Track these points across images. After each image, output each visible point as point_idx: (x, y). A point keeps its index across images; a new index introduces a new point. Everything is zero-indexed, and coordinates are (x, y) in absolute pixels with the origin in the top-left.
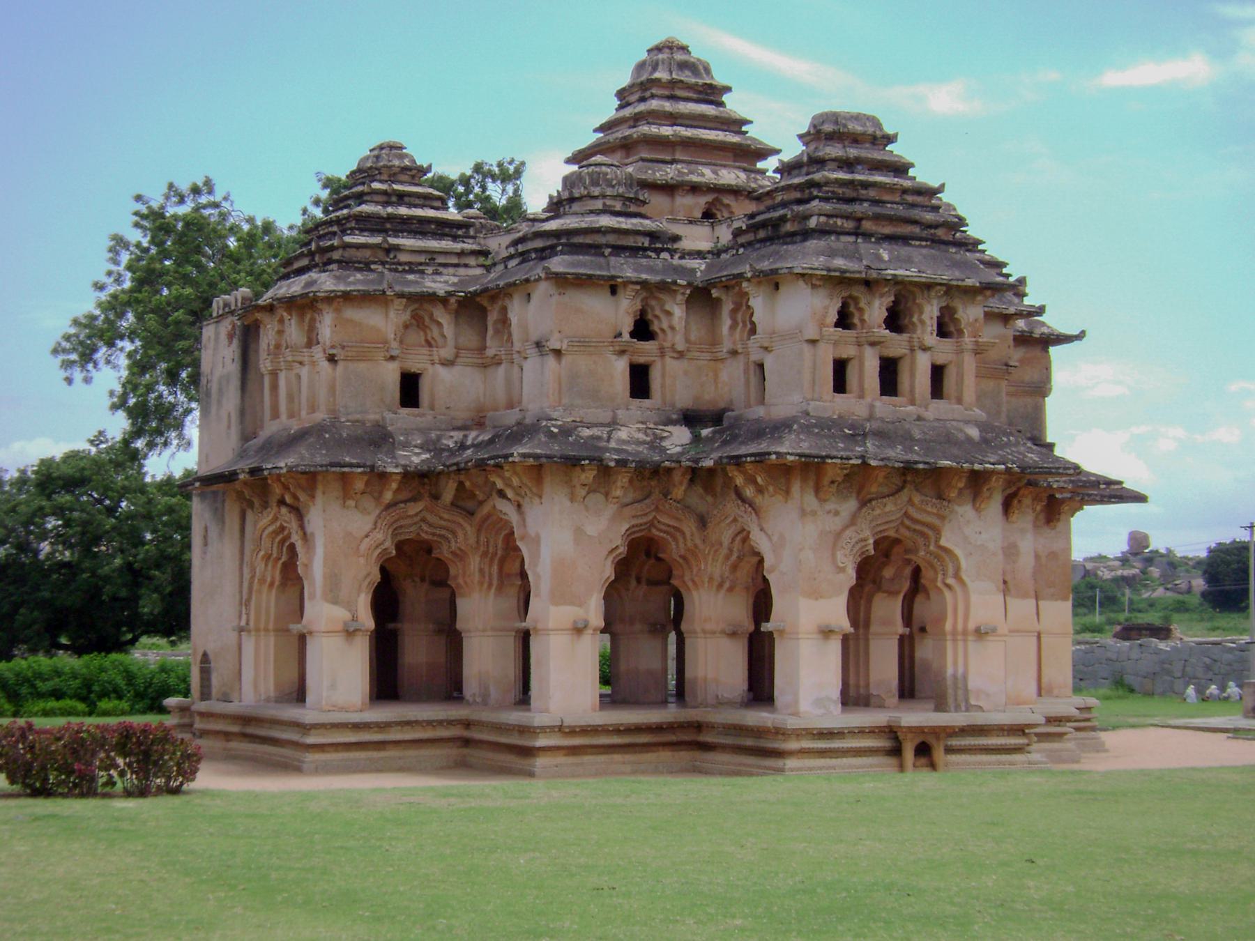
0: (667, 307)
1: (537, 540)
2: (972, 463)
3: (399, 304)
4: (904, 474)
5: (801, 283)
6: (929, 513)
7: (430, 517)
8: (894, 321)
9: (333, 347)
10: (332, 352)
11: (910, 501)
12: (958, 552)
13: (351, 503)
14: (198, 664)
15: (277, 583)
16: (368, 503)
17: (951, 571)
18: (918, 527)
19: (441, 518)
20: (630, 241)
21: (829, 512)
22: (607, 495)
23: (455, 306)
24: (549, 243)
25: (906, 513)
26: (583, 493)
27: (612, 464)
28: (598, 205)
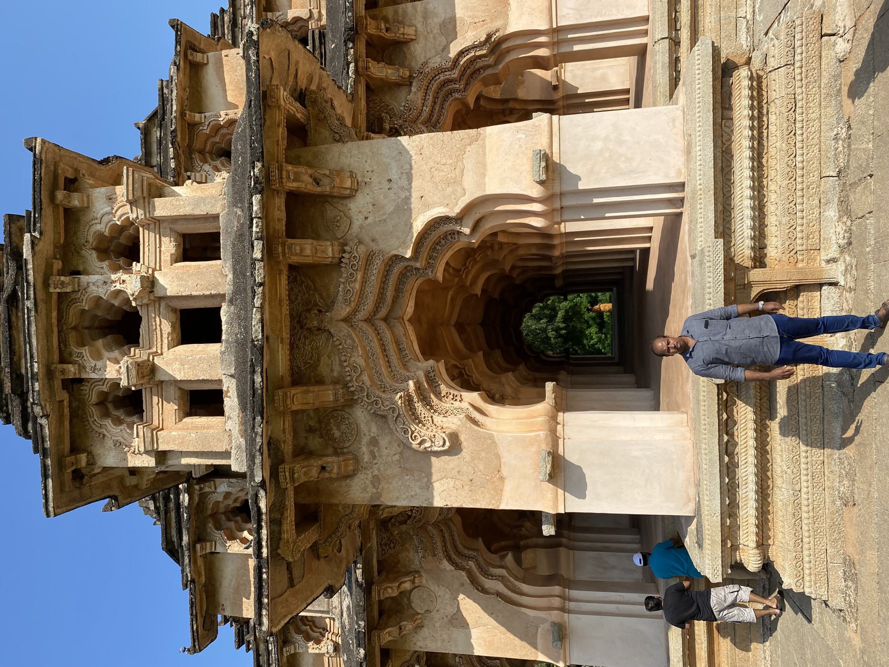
0: (220, 499)
2: (254, 261)
3: (289, 650)
4: (310, 329)
6: (364, 282)
8: (124, 326)
11: (347, 320)
12: (419, 224)
17: (451, 227)
18: (390, 294)
20: (173, 514)
21: (372, 453)
22: (411, 591)
25: (369, 320)
26: (408, 626)
27: (362, 651)
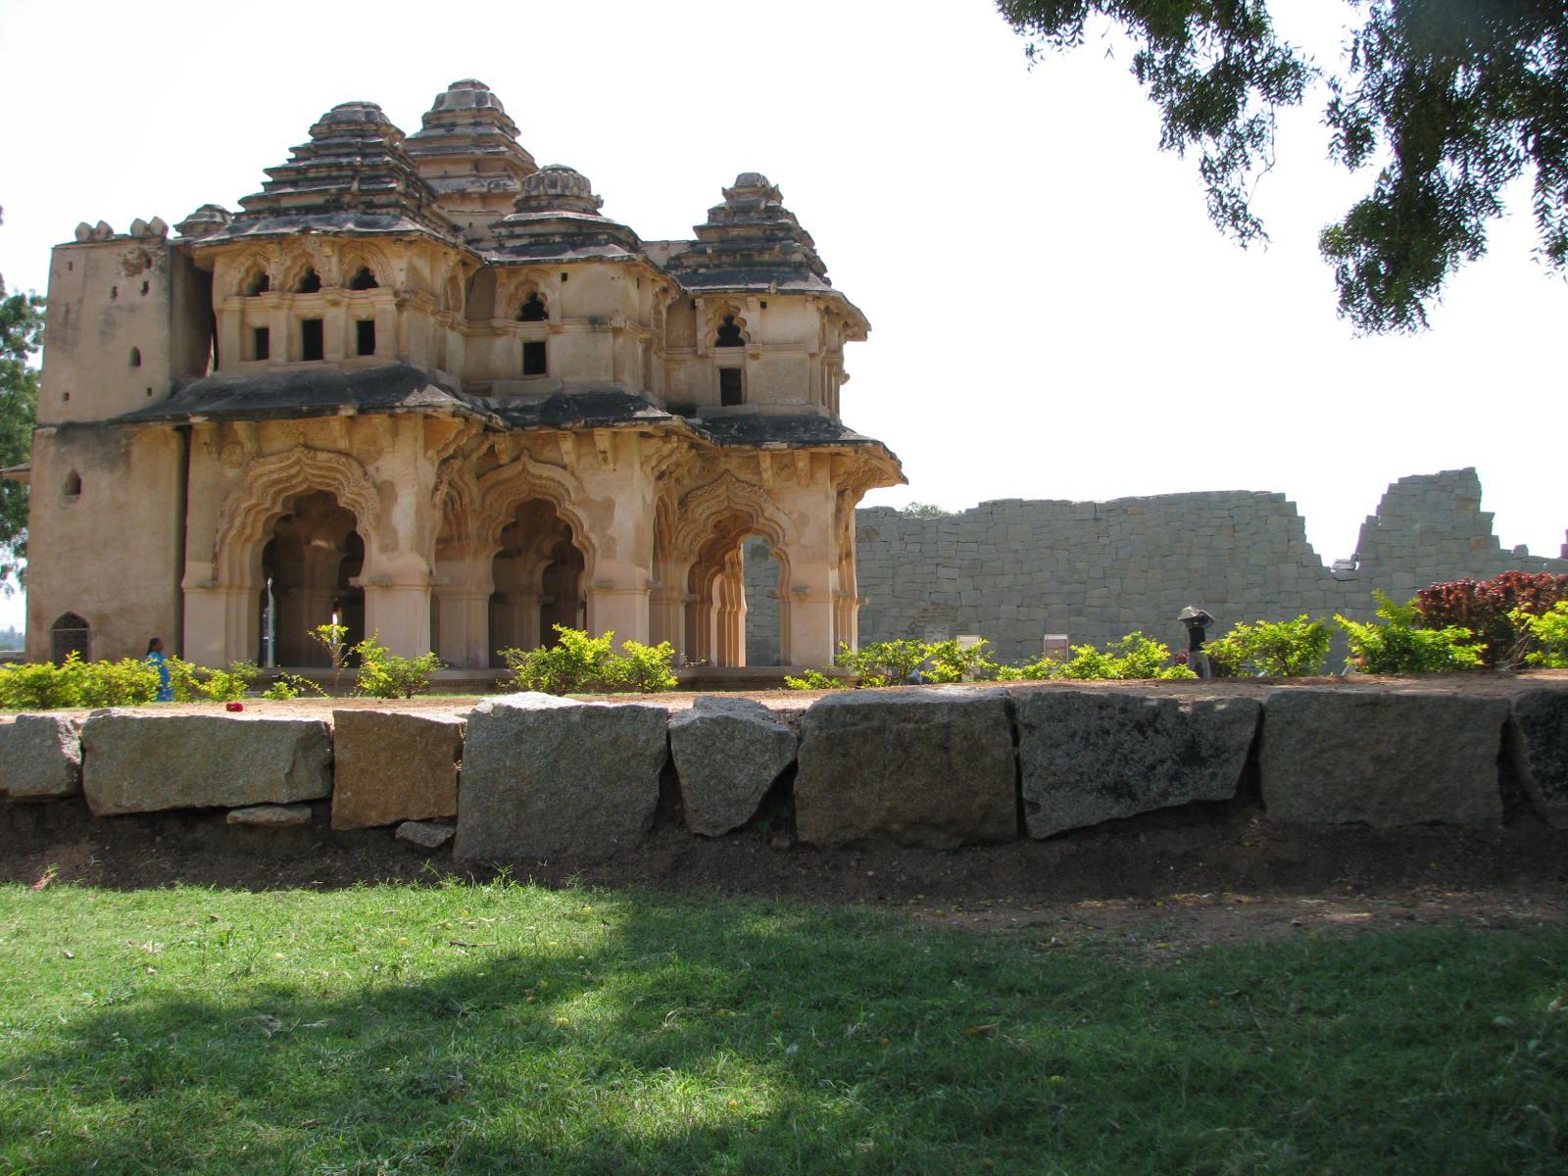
1: (608, 506)
5: (811, 307)
7: (457, 479)
9: (406, 292)
10: (407, 296)
13: (430, 453)
14: (49, 627)
15: (258, 536)
16: (435, 457)
19: (461, 478)
23: (471, 274)
24: (572, 230)
28: (583, 204)
